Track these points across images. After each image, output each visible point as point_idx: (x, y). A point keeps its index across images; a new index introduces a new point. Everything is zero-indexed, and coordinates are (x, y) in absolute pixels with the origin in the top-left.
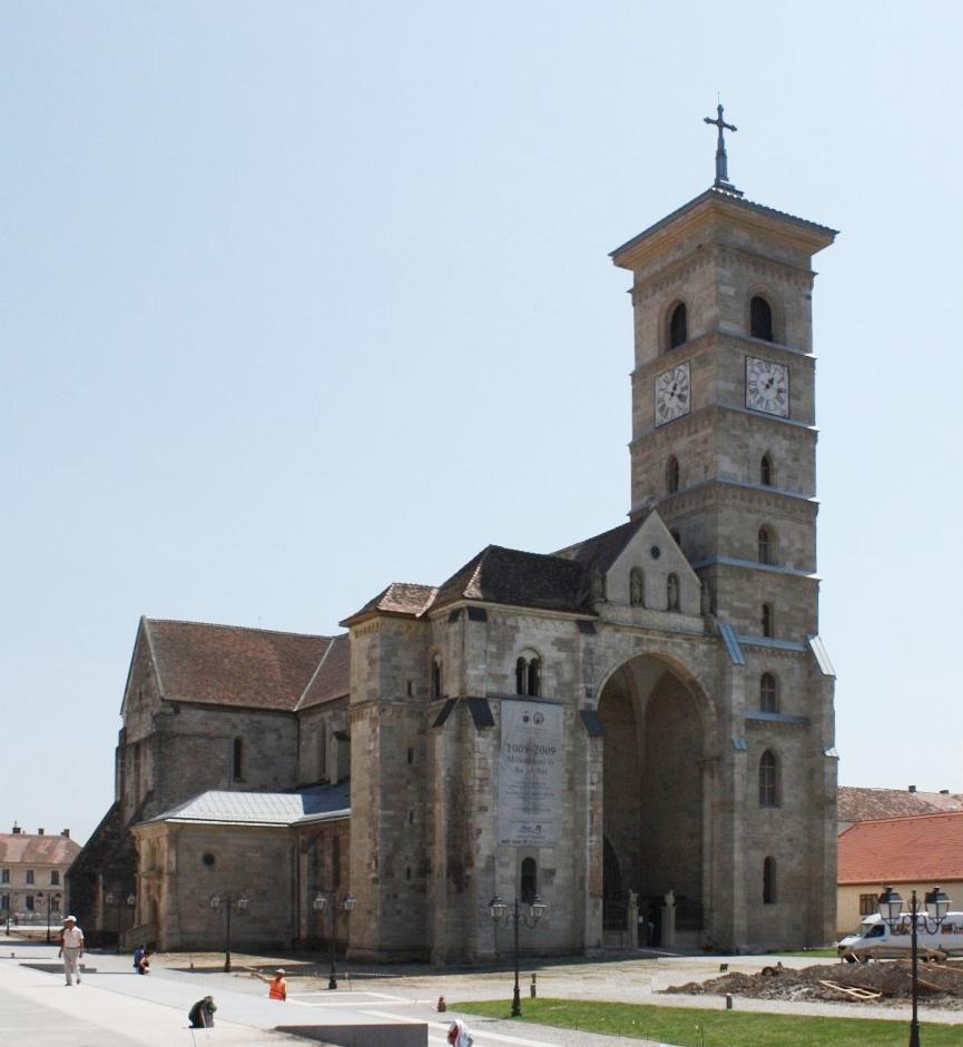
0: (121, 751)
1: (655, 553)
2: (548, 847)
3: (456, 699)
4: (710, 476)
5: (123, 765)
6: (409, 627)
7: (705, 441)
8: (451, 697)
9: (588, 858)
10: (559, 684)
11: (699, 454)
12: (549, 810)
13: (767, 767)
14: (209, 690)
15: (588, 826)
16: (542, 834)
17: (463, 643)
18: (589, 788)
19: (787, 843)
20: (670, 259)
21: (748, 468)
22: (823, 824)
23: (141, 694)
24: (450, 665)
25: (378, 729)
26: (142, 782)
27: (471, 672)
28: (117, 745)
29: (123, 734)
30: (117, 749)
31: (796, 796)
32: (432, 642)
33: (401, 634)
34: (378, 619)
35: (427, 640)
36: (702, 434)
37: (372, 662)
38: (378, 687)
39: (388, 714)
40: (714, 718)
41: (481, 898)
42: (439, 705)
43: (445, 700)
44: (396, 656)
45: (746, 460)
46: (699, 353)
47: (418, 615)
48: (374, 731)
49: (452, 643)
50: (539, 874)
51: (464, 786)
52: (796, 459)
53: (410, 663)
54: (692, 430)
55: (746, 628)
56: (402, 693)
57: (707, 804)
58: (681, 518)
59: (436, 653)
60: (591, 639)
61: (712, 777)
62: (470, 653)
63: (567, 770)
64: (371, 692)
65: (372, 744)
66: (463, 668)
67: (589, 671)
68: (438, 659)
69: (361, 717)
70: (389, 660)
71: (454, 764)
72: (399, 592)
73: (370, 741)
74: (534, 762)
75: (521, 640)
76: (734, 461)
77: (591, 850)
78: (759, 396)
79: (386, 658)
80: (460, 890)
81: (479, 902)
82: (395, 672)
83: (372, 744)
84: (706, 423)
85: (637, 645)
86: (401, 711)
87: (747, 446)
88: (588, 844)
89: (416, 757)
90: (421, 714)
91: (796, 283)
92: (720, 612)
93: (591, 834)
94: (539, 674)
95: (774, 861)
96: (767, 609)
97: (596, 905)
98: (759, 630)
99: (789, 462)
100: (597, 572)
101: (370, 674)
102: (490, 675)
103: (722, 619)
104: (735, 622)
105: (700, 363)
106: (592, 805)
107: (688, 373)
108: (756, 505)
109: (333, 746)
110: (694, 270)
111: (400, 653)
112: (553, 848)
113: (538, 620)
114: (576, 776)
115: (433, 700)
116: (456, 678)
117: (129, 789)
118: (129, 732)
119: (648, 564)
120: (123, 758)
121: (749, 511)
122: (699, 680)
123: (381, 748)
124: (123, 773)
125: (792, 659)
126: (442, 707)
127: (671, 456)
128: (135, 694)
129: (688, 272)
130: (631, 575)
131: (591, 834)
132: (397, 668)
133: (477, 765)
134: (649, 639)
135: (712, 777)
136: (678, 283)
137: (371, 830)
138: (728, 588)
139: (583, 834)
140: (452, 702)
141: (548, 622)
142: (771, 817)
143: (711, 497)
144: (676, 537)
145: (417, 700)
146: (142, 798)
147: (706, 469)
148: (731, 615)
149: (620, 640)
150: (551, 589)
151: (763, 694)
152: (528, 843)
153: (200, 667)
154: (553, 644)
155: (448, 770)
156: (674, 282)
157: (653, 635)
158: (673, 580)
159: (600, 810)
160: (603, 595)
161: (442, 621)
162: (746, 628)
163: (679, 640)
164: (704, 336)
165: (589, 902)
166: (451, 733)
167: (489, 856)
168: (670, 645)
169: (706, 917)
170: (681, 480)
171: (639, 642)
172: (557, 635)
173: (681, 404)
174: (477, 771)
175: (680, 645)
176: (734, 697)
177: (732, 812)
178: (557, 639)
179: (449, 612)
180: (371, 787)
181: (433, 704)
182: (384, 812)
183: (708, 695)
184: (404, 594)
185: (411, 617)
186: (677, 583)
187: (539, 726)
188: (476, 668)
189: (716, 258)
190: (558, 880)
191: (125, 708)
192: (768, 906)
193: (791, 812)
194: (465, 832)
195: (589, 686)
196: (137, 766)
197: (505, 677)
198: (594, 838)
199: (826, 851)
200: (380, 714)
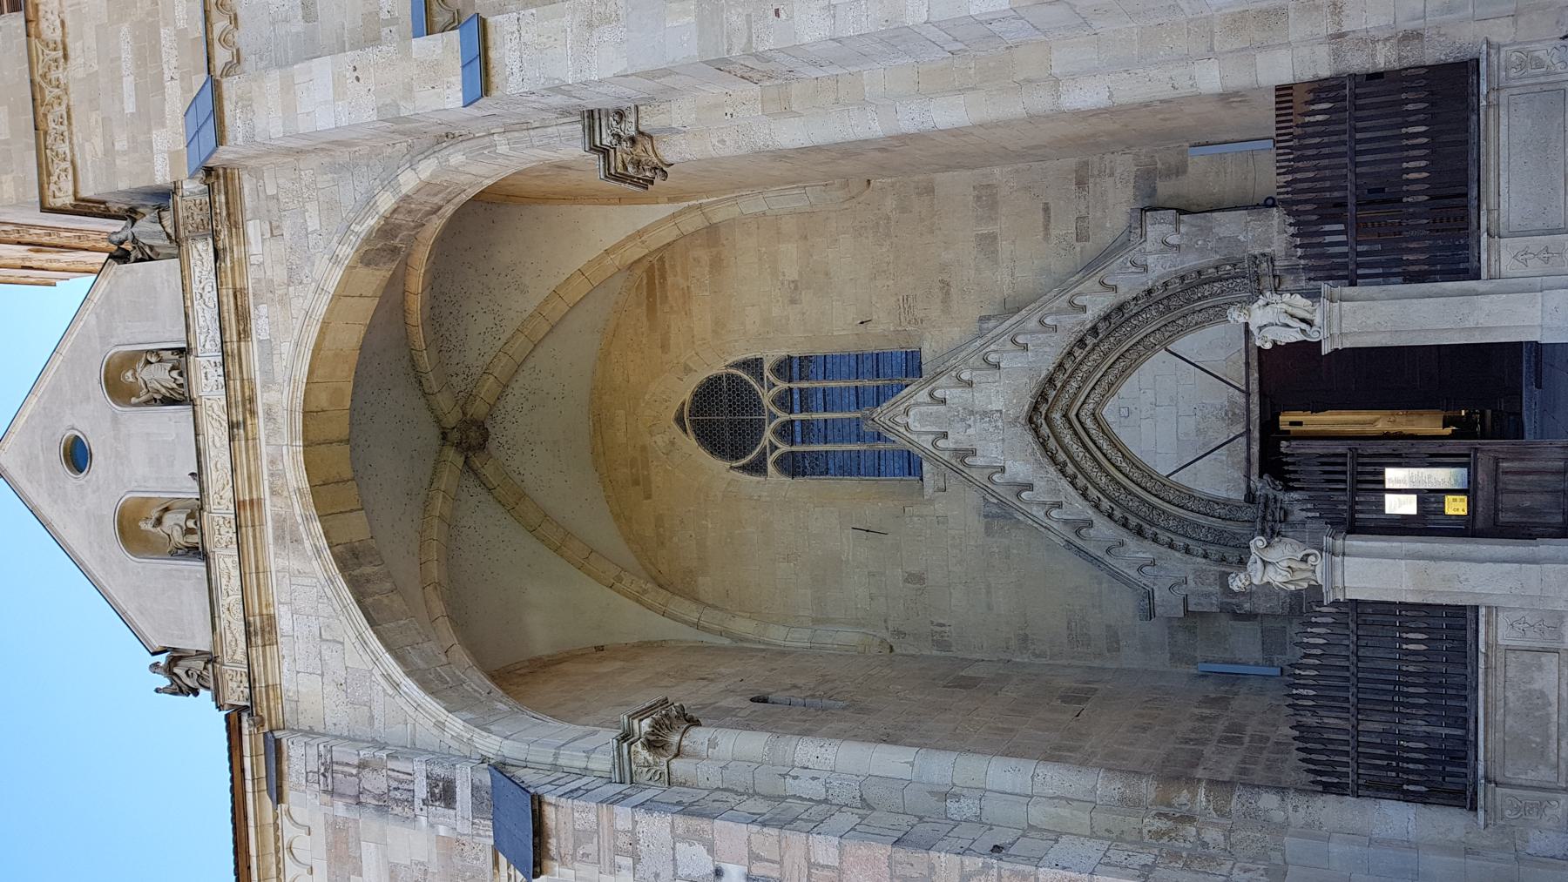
40: (456, 158)
60: (299, 758)
61: (672, 131)
67: (375, 782)
85: (297, 540)
92: (161, 176)
122: (347, 252)
134: (273, 493)
138: (98, 142)
148: (163, 125)
163: (253, 353)
169: (1384, 58)
171: (287, 536)
175: (268, 348)
183: (386, 202)
186: (131, 360)
195: (421, 791)
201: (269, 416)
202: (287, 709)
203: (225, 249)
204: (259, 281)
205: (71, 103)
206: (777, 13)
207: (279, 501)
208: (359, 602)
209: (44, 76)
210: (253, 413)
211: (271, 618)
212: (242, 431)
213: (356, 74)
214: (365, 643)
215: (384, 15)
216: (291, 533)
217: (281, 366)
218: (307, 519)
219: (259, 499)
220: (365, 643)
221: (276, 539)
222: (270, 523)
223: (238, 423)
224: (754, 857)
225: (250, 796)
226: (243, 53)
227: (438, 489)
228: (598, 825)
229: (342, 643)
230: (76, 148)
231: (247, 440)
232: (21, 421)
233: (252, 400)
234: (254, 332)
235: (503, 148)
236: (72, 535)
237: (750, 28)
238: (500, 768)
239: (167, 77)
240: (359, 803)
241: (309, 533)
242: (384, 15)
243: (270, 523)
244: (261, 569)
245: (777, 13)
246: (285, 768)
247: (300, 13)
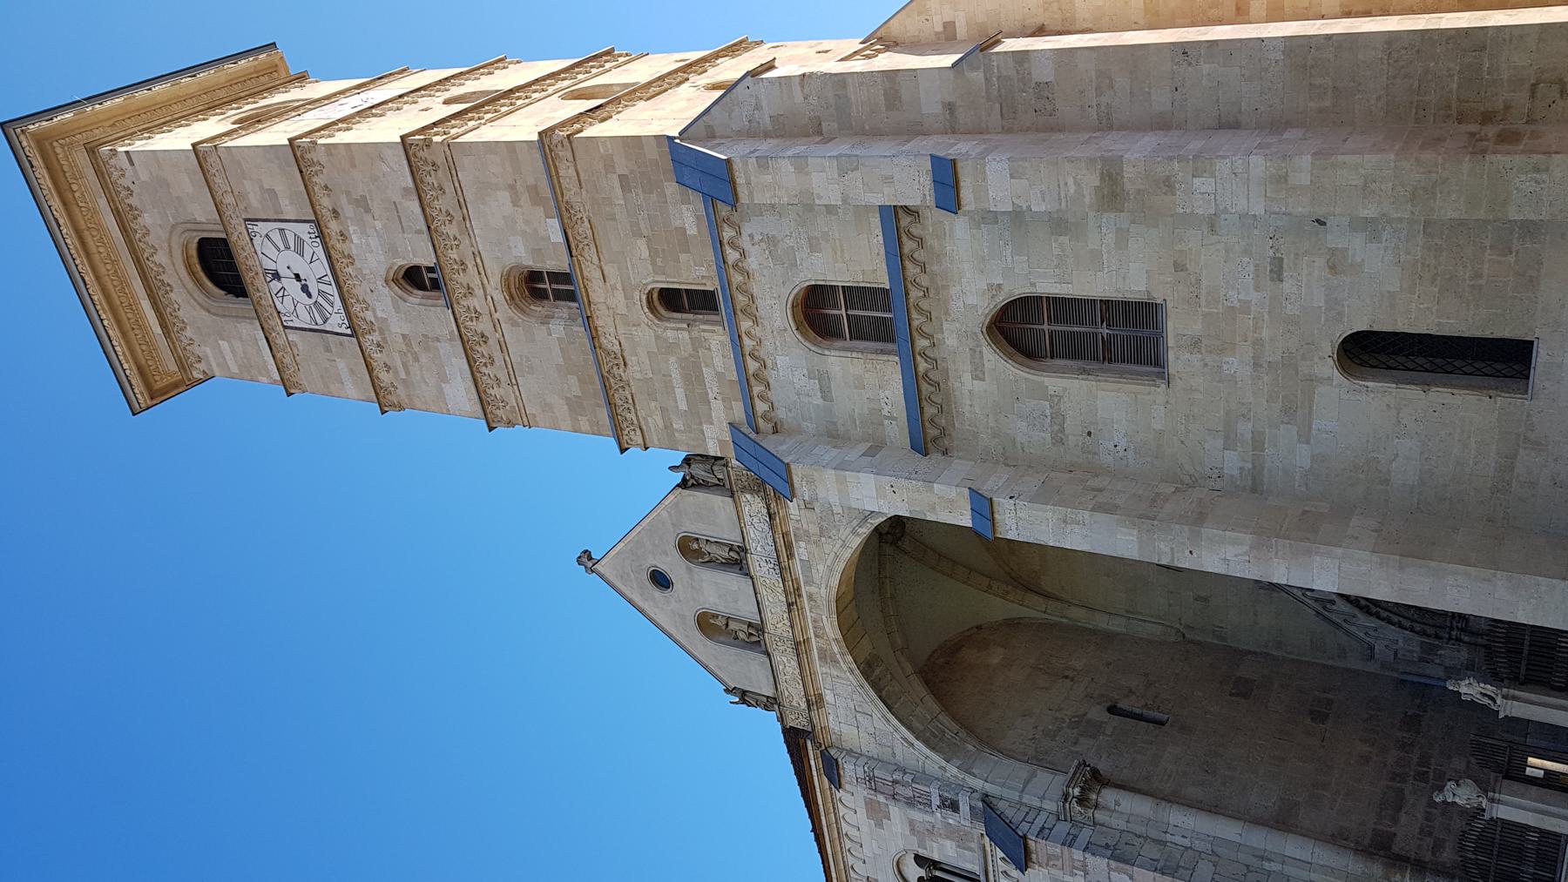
10: (947, 837)
19: (1288, 286)
31: (1122, 238)
45: (427, 342)
55: (720, 376)
60: (849, 770)
78: (320, 300)
103: (722, 443)
108: (484, 326)
121: (503, 346)
134: (816, 636)
142: (1195, 344)
154: (879, 825)
157: (804, 630)
168: (813, 589)
175: (808, 566)
193: (1179, 267)
195: (936, 801)
201: (810, 597)
202: (833, 737)
203: (775, 513)
204: (798, 529)
205: (633, 392)
206: (1191, 552)
208: (880, 697)
209: (609, 372)
210: (800, 596)
211: (820, 695)
212: (795, 607)
213: (893, 489)
214: (888, 721)
215: (885, 412)
216: (831, 657)
218: (843, 654)
219: (808, 638)
220: (888, 721)
221: (820, 658)
222: (815, 650)
223: (793, 603)
225: (816, 779)
226: (775, 404)
227: (886, 578)
228: (1062, 853)
229: (871, 716)
230: (641, 420)
231: (798, 610)
232: (613, 553)
233: (799, 589)
234: (796, 553)
236: (660, 619)
237: (1173, 554)
238: (985, 798)
239: (711, 396)
240: (894, 798)
241: (845, 662)
242: (885, 412)
243: (815, 650)
244: (812, 672)
245: (1191, 552)
246: (842, 773)
247: (819, 394)
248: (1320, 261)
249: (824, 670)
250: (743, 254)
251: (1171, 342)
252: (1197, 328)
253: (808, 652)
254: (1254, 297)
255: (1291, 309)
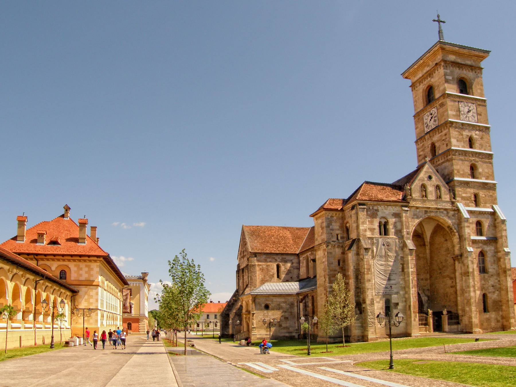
0: (238, 272)
1: (430, 178)
2: (395, 294)
3: (355, 239)
4: (448, 148)
5: (239, 276)
6: (336, 214)
7: (446, 135)
8: (353, 239)
9: (412, 298)
11: (443, 140)
12: (395, 280)
13: (481, 258)
14: (267, 248)
15: (411, 285)
16: (392, 290)
17: (357, 217)
18: (410, 270)
19: (492, 288)
20: (425, 71)
21: (464, 143)
22: (507, 279)
23: (243, 251)
24: (352, 224)
25: (326, 254)
26: (245, 282)
27: (361, 228)
28: (236, 270)
29: (239, 266)
30: (237, 271)
31: (494, 269)
32: (345, 219)
33: (333, 217)
34: (324, 212)
35: (343, 218)
36: (444, 132)
37: (322, 228)
38: (325, 237)
39: (330, 247)
41: (369, 316)
42: (349, 242)
43: (351, 240)
44: (331, 225)
46: (440, 102)
47: (339, 209)
48: (324, 254)
49: (353, 218)
50: (392, 305)
51: (361, 272)
52: (482, 138)
53: (338, 227)
54: (440, 132)
56: (335, 239)
57: (457, 274)
58: (439, 165)
59: (347, 222)
62: (361, 221)
63: (401, 264)
64: (323, 240)
65: (324, 259)
66: (358, 227)
67: (407, 225)
68: (348, 225)
69: (319, 249)
70: (329, 227)
71: (356, 264)
72: (332, 201)
73: (323, 258)
74: (388, 261)
75: (380, 214)
76: (457, 141)
77: (412, 294)
79: (328, 226)
80: (361, 313)
81: (369, 317)
82: (332, 231)
83: (324, 259)
84: (445, 128)
86: (335, 246)
87: (462, 135)
88: (411, 292)
89: (341, 263)
90: (342, 246)
91: (475, 72)
92: (458, 199)
93: (412, 288)
94: (388, 228)
95: (486, 295)
96: (476, 196)
97: (415, 316)
98: (473, 205)
99: (479, 139)
100: (409, 187)
101: (322, 233)
102: (369, 229)
104: (464, 202)
105: (441, 106)
106: (412, 277)
107: (436, 111)
109: (311, 264)
110: (435, 73)
111: (333, 224)
112: (397, 294)
113: (386, 207)
114: (405, 265)
115: (347, 241)
116: (355, 231)
117: (241, 285)
118: (240, 265)
119: (428, 183)
120: (239, 274)
123: (328, 260)
124: (238, 279)
125: (488, 215)
126: (350, 243)
127: (432, 143)
128: (242, 251)
129: (432, 74)
130: (421, 187)
131: (412, 288)
132: (332, 230)
133: (365, 264)
134: (430, 211)
135: (459, 263)
136: (429, 79)
137: (325, 292)
139: (409, 288)
140: (354, 241)
141: (390, 207)
143: (450, 155)
144: (438, 172)
145: (341, 241)
146: (245, 287)
147: (447, 145)
148: (462, 200)
149: (419, 212)
150: (390, 195)
151: (477, 229)
152: (387, 293)
153: (264, 240)
154: (393, 215)
155: (354, 266)
156: (427, 79)
158: (438, 188)
159: (415, 279)
160: (411, 195)
161: (349, 210)
162: (468, 203)
163: (442, 210)
164: (441, 96)
165: (413, 315)
166: (355, 252)
167: (372, 299)
168: (438, 212)
170: (437, 151)
172: (394, 212)
173: (434, 123)
174: (365, 266)
175: (442, 212)
176: (466, 231)
177: (468, 276)
178: (394, 213)
179: (351, 206)
180: (324, 275)
181: (347, 242)
182: (330, 285)
183: (455, 231)
184: (334, 202)
185: (336, 210)
187: (389, 247)
188: (363, 226)
189: (443, 66)
190: (400, 307)
191: (239, 257)
192: (486, 313)
193: (492, 275)
194: (362, 290)
196: (243, 276)
197: (374, 229)
198: (414, 289)
199: (509, 290)
200: (327, 247)
207: (429, 212)
217: (441, 214)
224: (414, 272)
235: (459, 246)
248: (494, 291)
249: (423, 211)
250: (486, 214)
251: (484, 274)
252: (486, 277)
253: (427, 209)
254: (490, 284)
255: (489, 288)
